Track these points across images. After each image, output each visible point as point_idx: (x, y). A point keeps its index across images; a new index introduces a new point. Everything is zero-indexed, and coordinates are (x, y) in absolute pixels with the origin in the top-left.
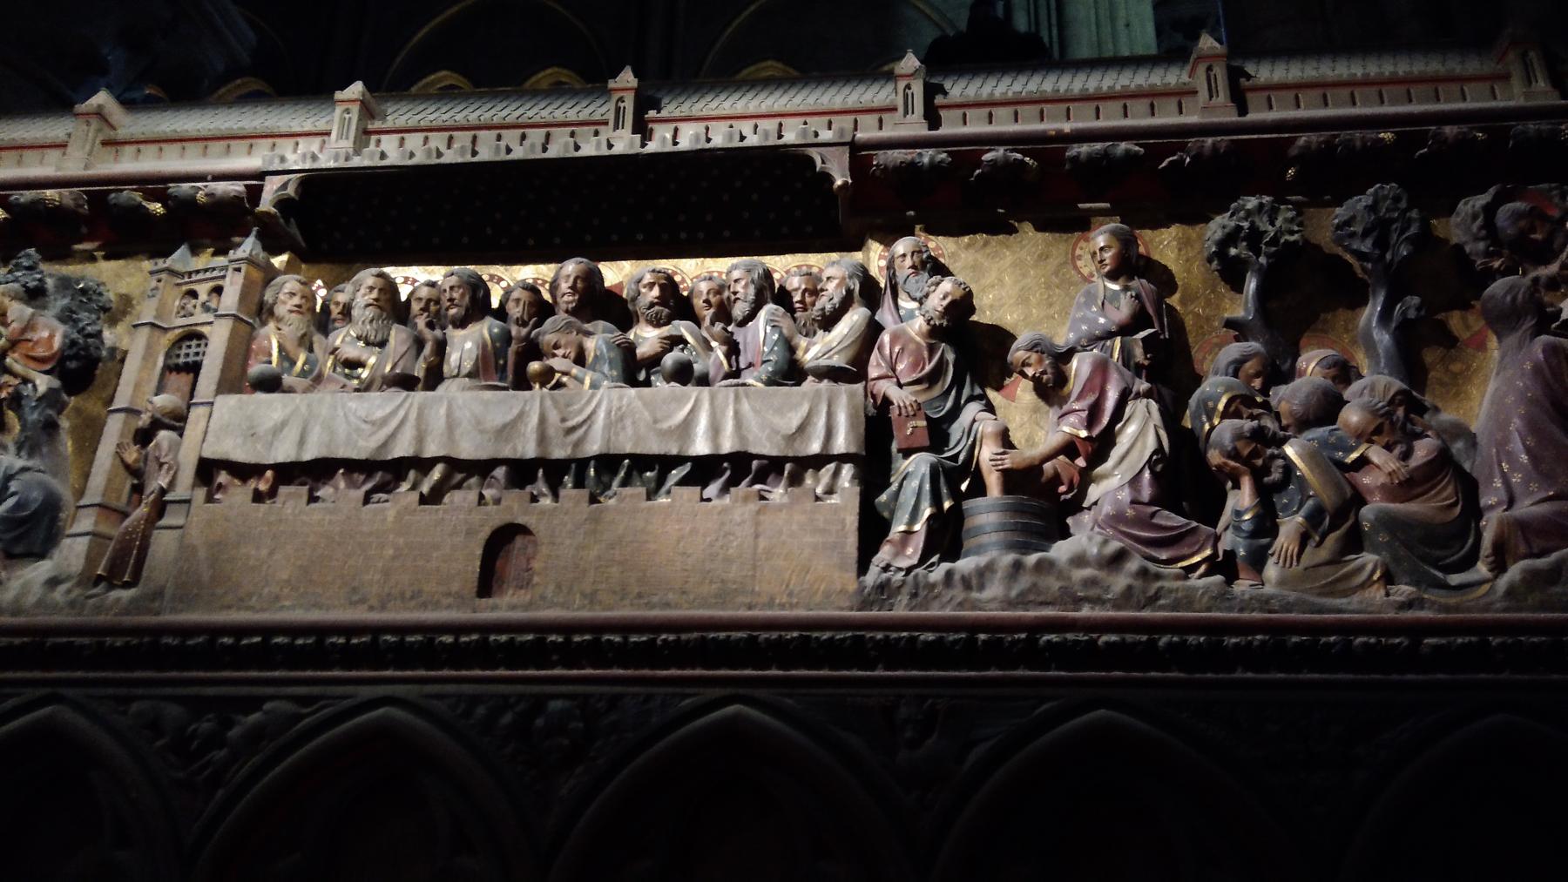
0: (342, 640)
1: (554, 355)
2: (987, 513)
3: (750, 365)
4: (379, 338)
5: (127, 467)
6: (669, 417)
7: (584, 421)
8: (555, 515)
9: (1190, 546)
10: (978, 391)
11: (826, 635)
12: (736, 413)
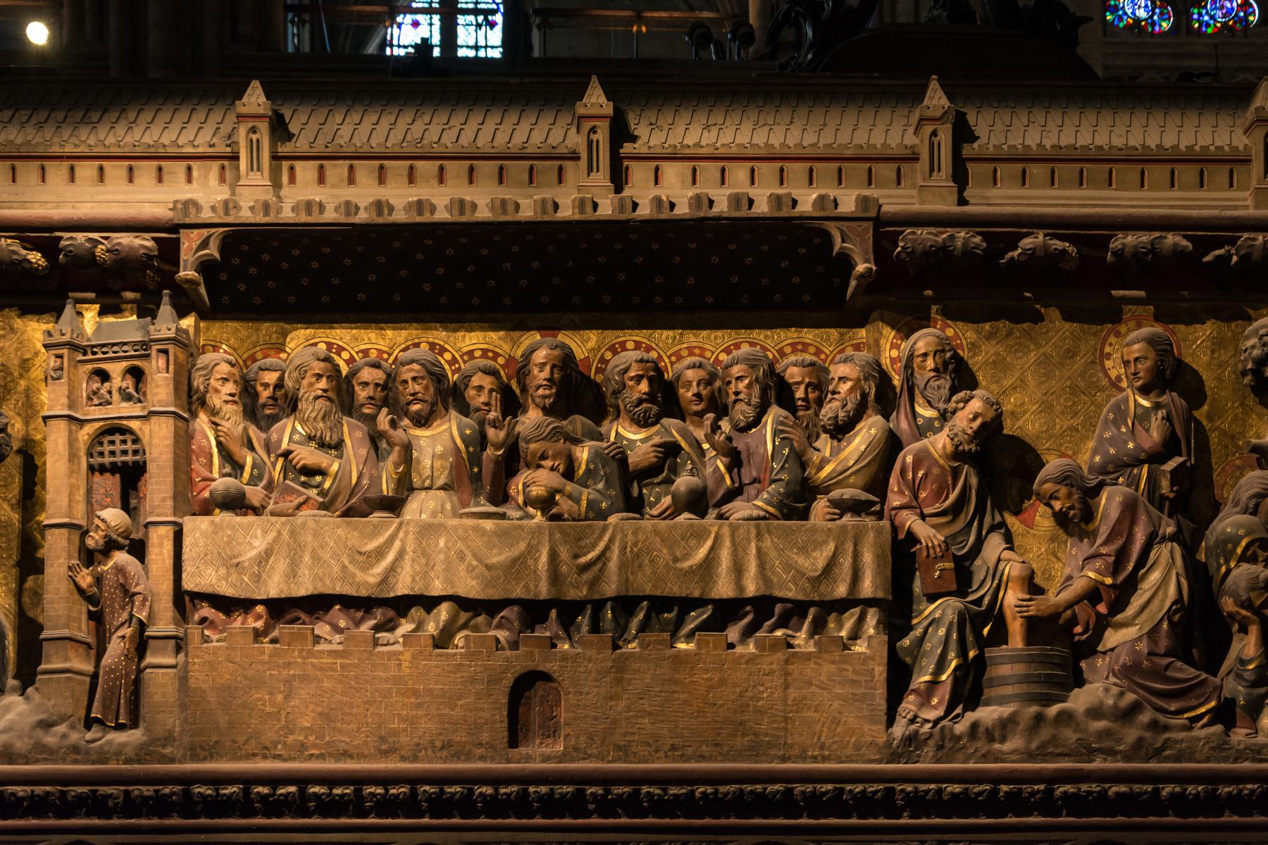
0: (380, 791)
1: (539, 466)
2: (1010, 661)
3: (755, 481)
4: (335, 438)
5: (81, 591)
6: (687, 556)
7: (599, 558)
8: (571, 654)
9: (1197, 698)
10: (998, 518)
11: (859, 788)
12: (759, 550)
